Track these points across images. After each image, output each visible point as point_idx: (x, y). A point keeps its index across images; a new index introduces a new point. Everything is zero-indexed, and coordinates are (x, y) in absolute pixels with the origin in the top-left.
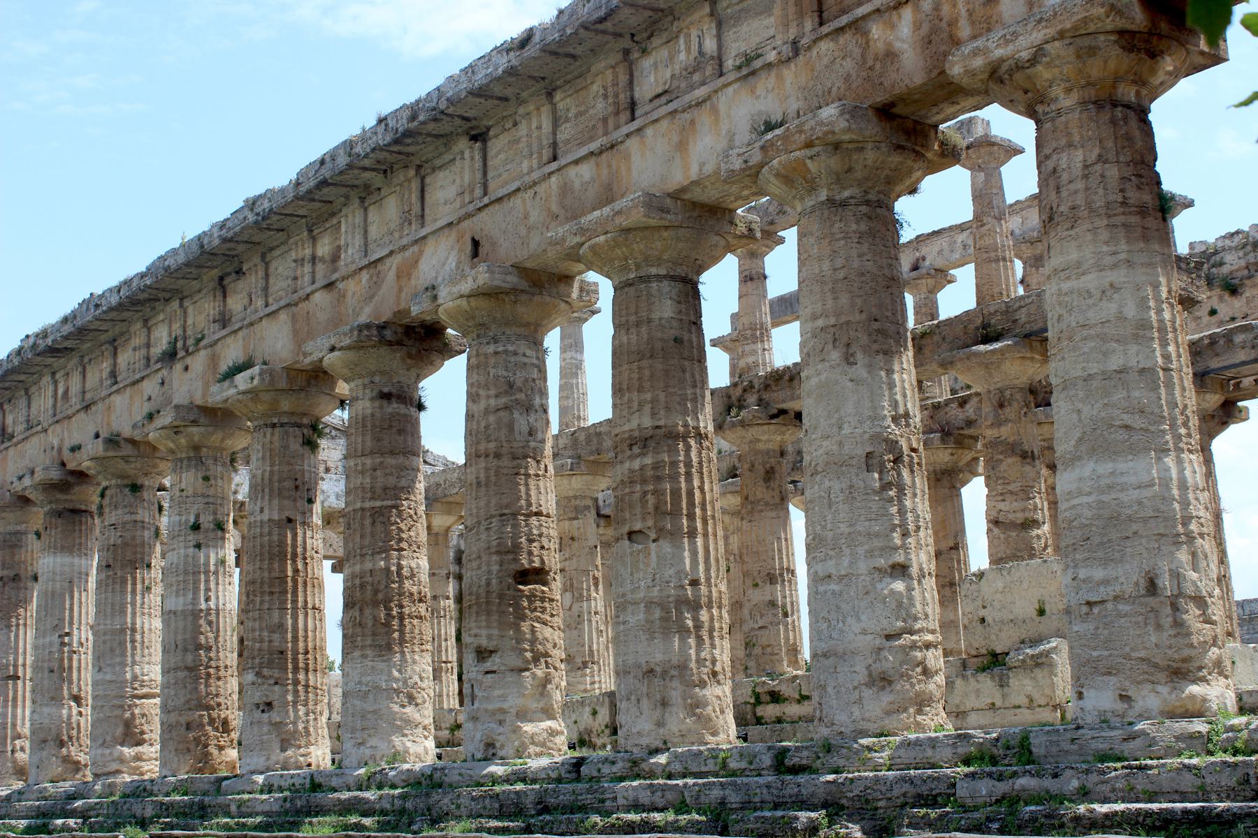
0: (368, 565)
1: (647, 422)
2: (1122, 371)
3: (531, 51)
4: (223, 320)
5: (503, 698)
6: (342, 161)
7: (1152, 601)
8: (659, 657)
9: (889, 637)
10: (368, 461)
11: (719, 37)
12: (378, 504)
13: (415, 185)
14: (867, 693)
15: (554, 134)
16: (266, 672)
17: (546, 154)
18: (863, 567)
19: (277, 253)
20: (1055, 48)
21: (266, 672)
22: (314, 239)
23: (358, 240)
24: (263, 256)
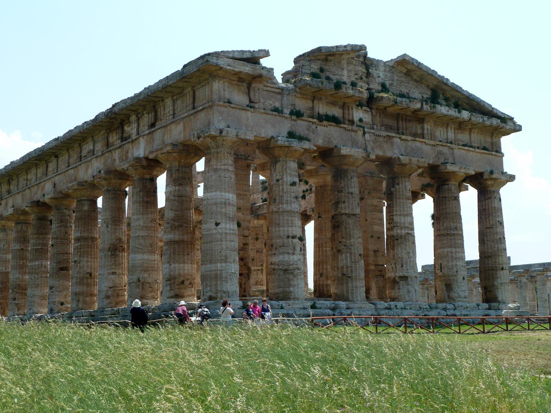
0: (34, 264)
1: (79, 235)
2: (139, 236)
3: (59, 142)
4: (9, 192)
5: (55, 298)
6: (27, 158)
7: (138, 283)
8: (78, 290)
9: (110, 288)
10: (35, 236)
11: (94, 146)
12: (37, 247)
13: (45, 165)
14: (105, 300)
15: (69, 160)
16: (14, 290)
17: (67, 165)
18: (106, 272)
19: (20, 176)
20: (130, 168)
21: (14, 290)
22: (27, 174)
23: (34, 177)
24: (17, 176)
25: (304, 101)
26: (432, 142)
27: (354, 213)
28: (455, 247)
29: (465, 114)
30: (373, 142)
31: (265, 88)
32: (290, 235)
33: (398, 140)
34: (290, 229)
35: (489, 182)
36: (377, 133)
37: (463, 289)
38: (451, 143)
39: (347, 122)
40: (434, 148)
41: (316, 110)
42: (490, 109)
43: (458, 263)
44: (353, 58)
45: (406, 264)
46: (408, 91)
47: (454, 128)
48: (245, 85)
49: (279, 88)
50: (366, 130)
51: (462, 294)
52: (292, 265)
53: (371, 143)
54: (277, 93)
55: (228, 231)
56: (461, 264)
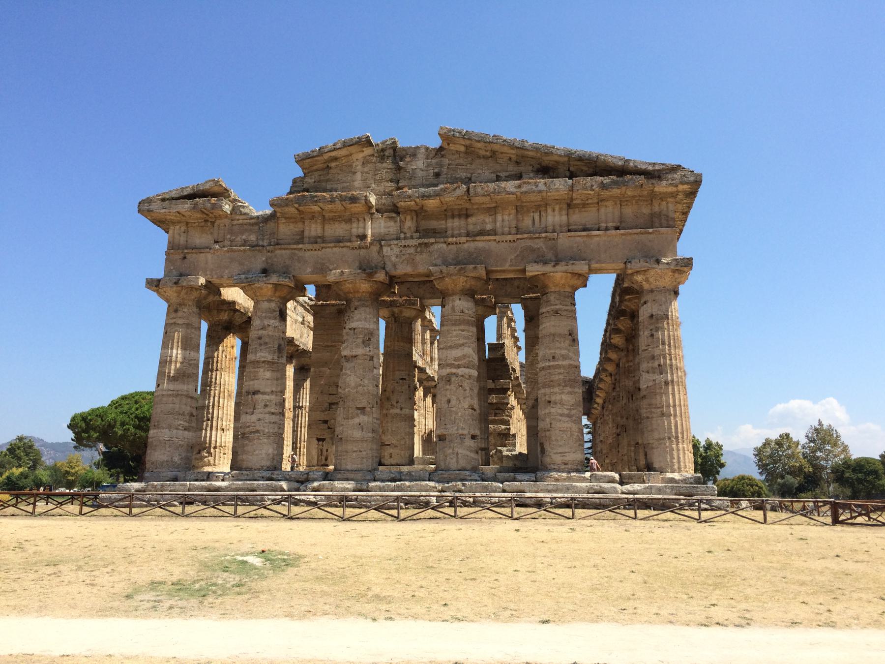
25: (292, 226)
26: (509, 237)
27: (354, 354)
28: (549, 386)
29: (560, 185)
30: (397, 257)
31: (235, 222)
32: (251, 389)
33: (445, 246)
34: (252, 383)
35: (639, 278)
36: (403, 243)
37: (560, 450)
38: (554, 231)
39: (354, 239)
40: (515, 244)
41: (306, 233)
42: (620, 163)
43: (553, 410)
44: (373, 155)
45: (445, 416)
46: (469, 175)
47: (561, 209)
48: (209, 224)
49: (252, 218)
50: (383, 243)
51: (558, 459)
52: (249, 427)
53: (393, 258)
54: (252, 224)
55: (164, 393)
56: (560, 411)
